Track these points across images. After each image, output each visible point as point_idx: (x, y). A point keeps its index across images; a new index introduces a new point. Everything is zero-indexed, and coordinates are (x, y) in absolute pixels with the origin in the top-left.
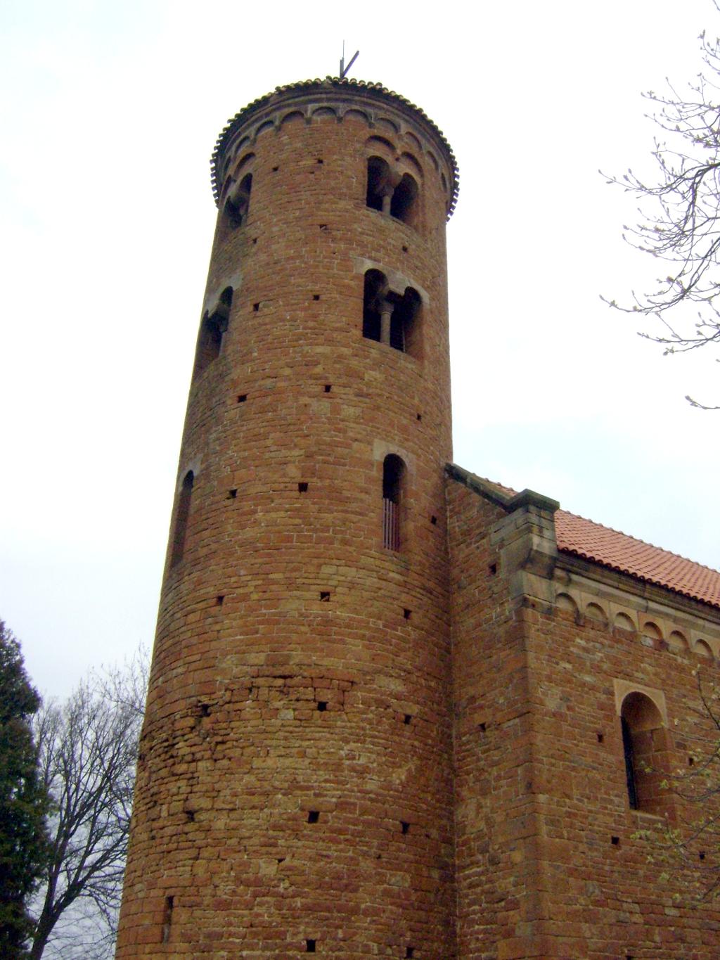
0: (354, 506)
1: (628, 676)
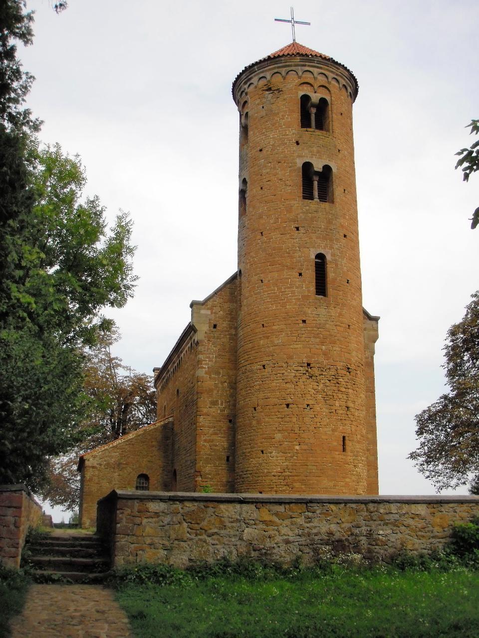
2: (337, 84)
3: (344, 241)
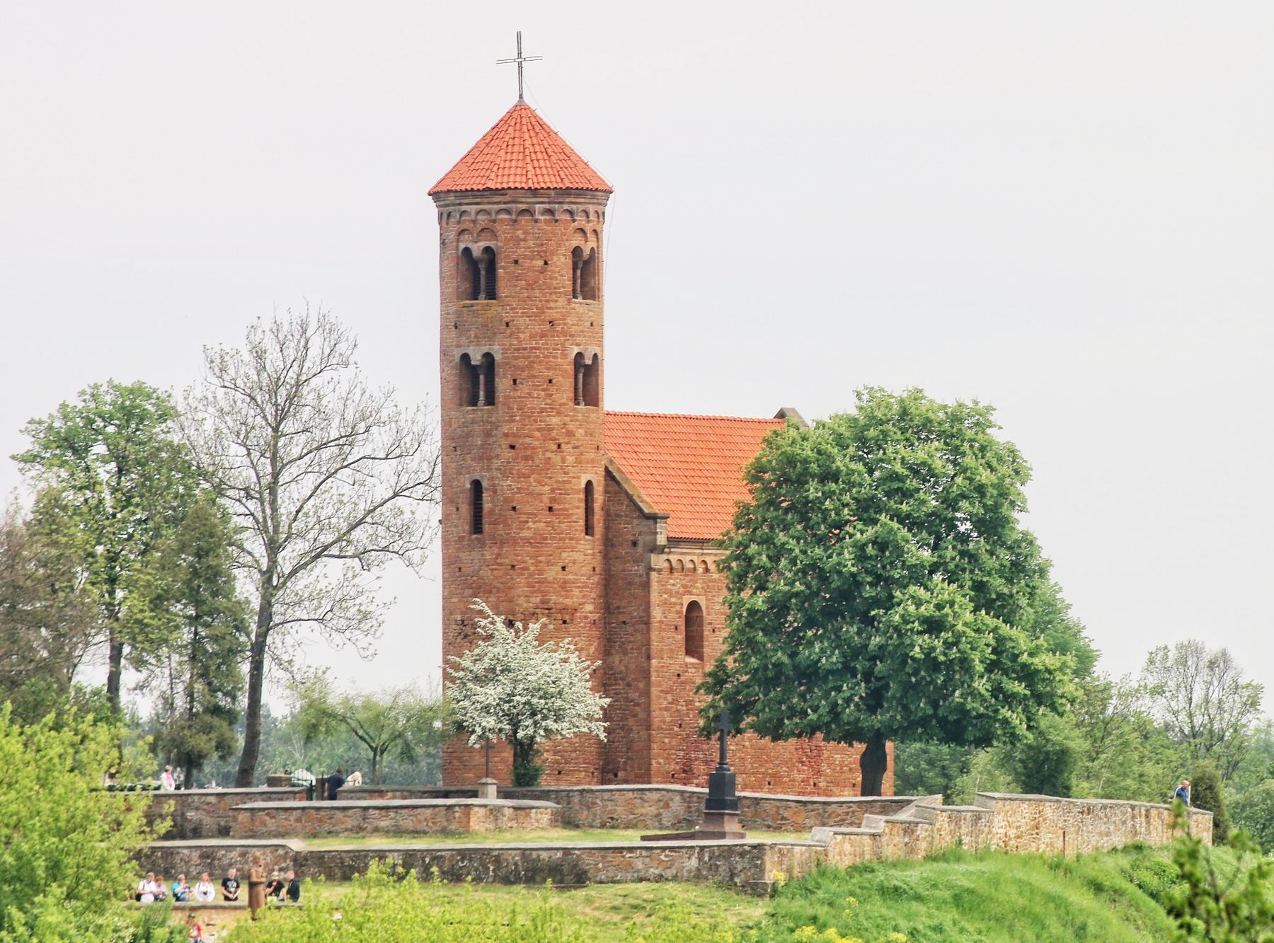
0: (574, 518)
1: (690, 593)
2: (507, 217)
3: (507, 454)
